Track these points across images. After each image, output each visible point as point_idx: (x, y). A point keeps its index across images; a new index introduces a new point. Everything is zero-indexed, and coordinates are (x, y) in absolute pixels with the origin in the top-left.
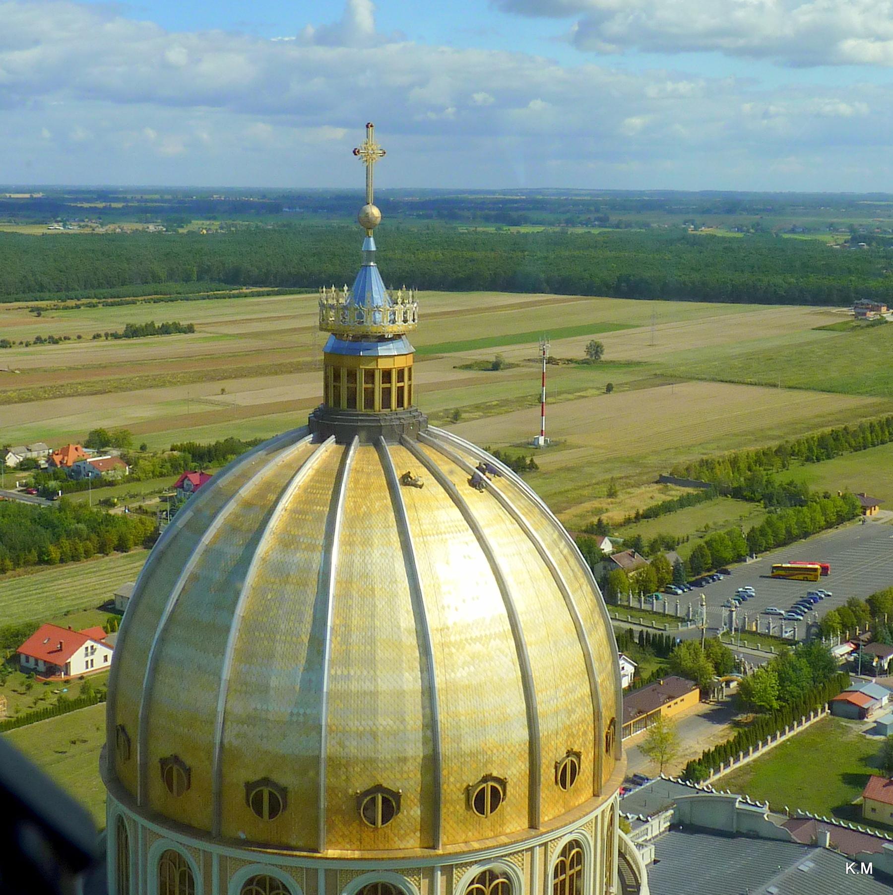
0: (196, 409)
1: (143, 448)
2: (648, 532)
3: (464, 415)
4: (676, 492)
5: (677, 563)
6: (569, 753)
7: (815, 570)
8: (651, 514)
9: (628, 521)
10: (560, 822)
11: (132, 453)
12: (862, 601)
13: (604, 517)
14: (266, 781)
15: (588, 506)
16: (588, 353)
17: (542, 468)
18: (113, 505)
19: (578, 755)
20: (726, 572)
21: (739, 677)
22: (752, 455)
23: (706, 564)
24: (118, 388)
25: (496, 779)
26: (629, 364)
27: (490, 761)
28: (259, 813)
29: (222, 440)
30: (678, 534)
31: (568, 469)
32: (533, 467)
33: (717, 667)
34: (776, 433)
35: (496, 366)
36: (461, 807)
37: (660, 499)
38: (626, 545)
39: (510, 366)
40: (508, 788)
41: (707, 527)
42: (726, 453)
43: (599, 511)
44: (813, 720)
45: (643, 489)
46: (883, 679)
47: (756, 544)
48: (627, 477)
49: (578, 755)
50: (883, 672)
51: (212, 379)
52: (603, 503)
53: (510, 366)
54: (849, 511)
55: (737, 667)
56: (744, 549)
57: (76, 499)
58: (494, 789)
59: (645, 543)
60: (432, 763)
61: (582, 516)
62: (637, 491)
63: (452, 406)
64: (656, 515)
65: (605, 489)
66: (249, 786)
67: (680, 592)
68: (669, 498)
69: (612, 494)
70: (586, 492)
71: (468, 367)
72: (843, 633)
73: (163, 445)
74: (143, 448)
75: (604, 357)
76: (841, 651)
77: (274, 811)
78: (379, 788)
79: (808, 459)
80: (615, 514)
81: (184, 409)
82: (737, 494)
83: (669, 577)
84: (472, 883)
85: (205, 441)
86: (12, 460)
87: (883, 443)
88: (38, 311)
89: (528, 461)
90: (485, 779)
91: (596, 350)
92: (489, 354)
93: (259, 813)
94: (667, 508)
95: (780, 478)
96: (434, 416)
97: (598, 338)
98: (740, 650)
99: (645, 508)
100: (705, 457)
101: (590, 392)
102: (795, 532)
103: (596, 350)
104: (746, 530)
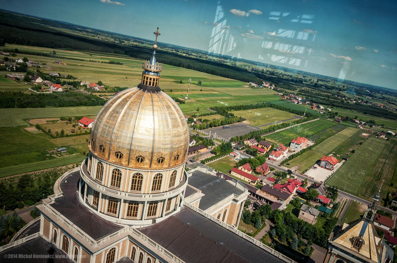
6: (177, 155)
10: (173, 167)
14: (119, 152)
19: (179, 156)
25: (163, 158)
27: (162, 154)
36: (155, 162)
40: (165, 160)
44: (226, 156)
46: (239, 151)
49: (179, 156)
50: (240, 150)
58: (162, 159)
60: (152, 153)
66: (116, 153)
76: (233, 145)
77: (120, 157)
78: (141, 156)
84: (135, 174)
86: (82, 84)
88: (91, 55)
90: (161, 157)
98: (215, 142)
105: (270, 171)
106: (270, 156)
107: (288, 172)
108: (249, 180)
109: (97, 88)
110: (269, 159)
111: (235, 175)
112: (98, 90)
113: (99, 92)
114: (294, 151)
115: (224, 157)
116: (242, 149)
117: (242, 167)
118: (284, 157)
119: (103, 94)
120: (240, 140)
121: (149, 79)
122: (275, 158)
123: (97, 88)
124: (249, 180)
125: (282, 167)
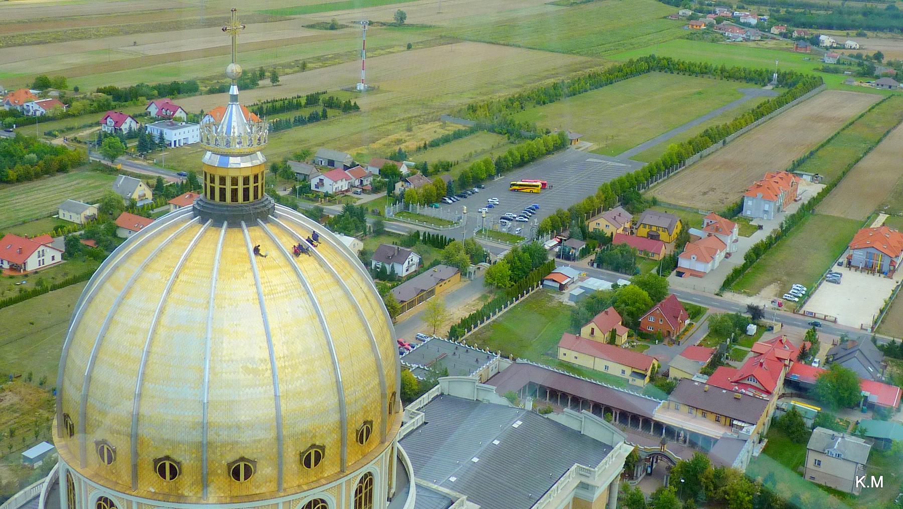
0: (114, 57)
1: (76, 90)
2: (432, 158)
3: (309, 65)
4: (453, 127)
5: (449, 183)
7: (537, 186)
8: (435, 144)
9: (419, 149)
11: (69, 93)
12: (566, 211)
13: (403, 146)
14: (167, 458)
15: (393, 137)
16: (396, 19)
17: (362, 109)
18: (55, 136)
20: (479, 187)
21: (485, 265)
22: (502, 99)
23: (468, 183)
24: (57, 40)
26: (423, 27)
28: (163, 474)
29: (135, 85)
30: (451, 159)
31: (381, 109)
32: (356, 108)
33: (471, 258)
34: (520, 83)
35: (333, 27)
37: (441, 133)
38: (416, 167)
39: (343, 27)
41: (471, 154)
42: (485, 98)
43: (399, 142)
45: (430, 125)
47: (502, 167)
48: (419, 116)
51: (127, 33)
52: (403, 135)
53: (343, 27)
54: (561, 145)
55: (484, 258)
56: (494, 172)
57: (26, 132)
59: (430, 169)
61: (388, 145)
62: (426, 126)
63: (301, 57)
64: (438, 145)
65: (404, 125)
66: (156, 461)
67: (450, 201)
68: (447, 132)
69: (409, 129)
70: (391, 127)
71: (312, 27)
72: (552, 232)
73: (90, 86)
74: (76, 90)
75: (406, 22)
76: (550, 243)
79: (538, 103)
80: (411, 145)
81: (105, 58)
82: (492, 130)
83: (444, 193)
85: (123, 83)
87: (586, 91)
89: (352, 104)
91: (401, 17)
92: (327, 16)
93: (163, 474)
94: (446, 140)
95: (519, 118)
96: (289, 66)
97: (403, 7)
98: (486, 243)
99: (430, 140)
100: (470, 101)
101: (396, 49)
102: (526, 158)
103: (401, 17)
104: (496, 157)
105: (688, 322)
106: (683, 263)
107: (749, 316)
108: (623, 372)
109: (36, 107)
110: (680, 274)
111: (573, 361)
112: (38, 114)
113: (43, 119)
114: (760, 227)
115: (526, 296)
116: (585, 253)
117: (592, 325)
118: (728, 255)
119: (63, 124)
120: (570, 224)
121: (228, 182)
122: (699, 267)
123: (35, 107)
124: (623, 372)
125: (728, 296)
